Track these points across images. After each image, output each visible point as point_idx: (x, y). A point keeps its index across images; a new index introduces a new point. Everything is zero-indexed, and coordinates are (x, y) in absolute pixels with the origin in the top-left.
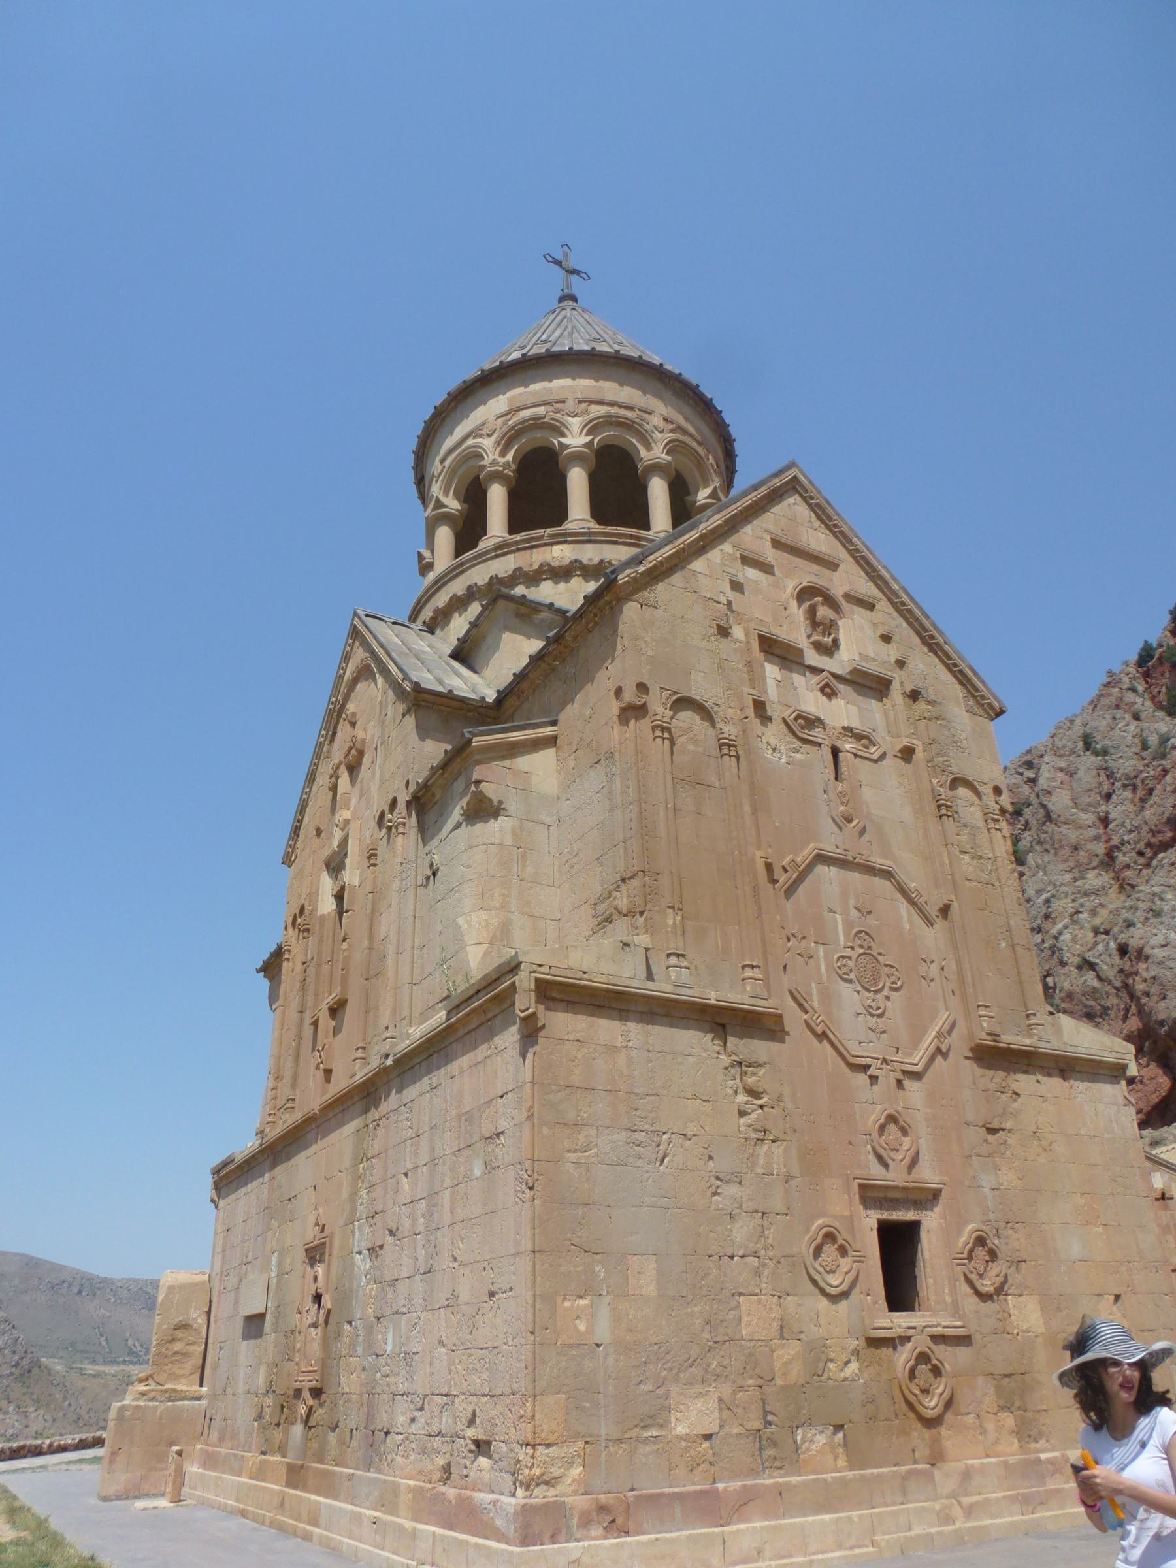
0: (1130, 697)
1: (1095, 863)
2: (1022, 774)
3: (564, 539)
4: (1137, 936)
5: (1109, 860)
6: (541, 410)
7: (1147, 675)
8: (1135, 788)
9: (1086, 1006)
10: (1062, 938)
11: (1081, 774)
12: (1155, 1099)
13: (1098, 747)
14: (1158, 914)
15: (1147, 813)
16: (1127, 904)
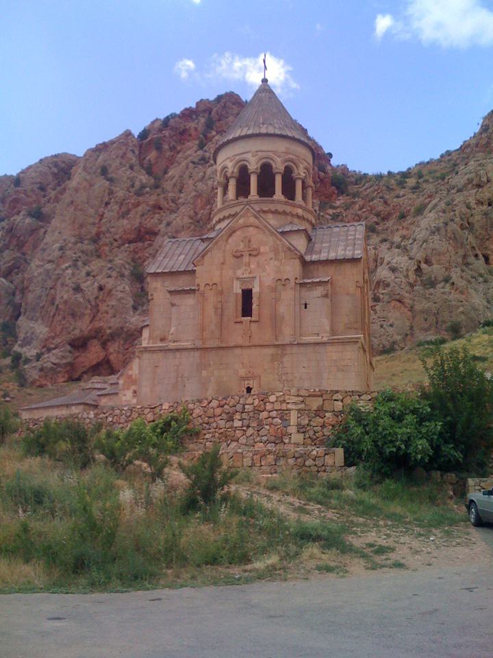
0: (130, 155)
1: (88, 237)
2: (51, 168)
3: (300, 207)
4: (111, 284)
5: (96, 239)
6: (294, 157)
7: (141, 146)
8: (122, 204)
9: (73, 310)
10: (67, 272)
11: (96, 187)
12: (94, 362)
13: (109, 176)
14: (123, 276)
15: (125, 222)
16: (109, 266)
